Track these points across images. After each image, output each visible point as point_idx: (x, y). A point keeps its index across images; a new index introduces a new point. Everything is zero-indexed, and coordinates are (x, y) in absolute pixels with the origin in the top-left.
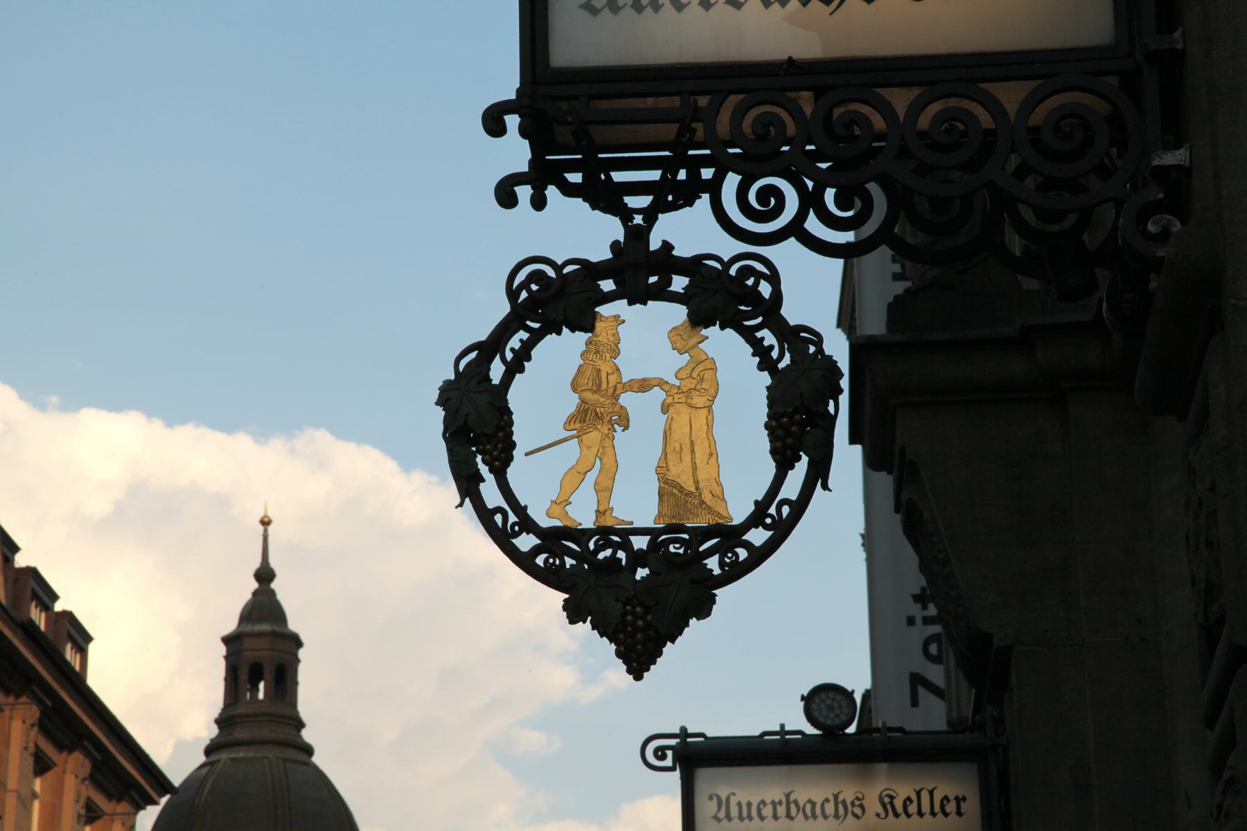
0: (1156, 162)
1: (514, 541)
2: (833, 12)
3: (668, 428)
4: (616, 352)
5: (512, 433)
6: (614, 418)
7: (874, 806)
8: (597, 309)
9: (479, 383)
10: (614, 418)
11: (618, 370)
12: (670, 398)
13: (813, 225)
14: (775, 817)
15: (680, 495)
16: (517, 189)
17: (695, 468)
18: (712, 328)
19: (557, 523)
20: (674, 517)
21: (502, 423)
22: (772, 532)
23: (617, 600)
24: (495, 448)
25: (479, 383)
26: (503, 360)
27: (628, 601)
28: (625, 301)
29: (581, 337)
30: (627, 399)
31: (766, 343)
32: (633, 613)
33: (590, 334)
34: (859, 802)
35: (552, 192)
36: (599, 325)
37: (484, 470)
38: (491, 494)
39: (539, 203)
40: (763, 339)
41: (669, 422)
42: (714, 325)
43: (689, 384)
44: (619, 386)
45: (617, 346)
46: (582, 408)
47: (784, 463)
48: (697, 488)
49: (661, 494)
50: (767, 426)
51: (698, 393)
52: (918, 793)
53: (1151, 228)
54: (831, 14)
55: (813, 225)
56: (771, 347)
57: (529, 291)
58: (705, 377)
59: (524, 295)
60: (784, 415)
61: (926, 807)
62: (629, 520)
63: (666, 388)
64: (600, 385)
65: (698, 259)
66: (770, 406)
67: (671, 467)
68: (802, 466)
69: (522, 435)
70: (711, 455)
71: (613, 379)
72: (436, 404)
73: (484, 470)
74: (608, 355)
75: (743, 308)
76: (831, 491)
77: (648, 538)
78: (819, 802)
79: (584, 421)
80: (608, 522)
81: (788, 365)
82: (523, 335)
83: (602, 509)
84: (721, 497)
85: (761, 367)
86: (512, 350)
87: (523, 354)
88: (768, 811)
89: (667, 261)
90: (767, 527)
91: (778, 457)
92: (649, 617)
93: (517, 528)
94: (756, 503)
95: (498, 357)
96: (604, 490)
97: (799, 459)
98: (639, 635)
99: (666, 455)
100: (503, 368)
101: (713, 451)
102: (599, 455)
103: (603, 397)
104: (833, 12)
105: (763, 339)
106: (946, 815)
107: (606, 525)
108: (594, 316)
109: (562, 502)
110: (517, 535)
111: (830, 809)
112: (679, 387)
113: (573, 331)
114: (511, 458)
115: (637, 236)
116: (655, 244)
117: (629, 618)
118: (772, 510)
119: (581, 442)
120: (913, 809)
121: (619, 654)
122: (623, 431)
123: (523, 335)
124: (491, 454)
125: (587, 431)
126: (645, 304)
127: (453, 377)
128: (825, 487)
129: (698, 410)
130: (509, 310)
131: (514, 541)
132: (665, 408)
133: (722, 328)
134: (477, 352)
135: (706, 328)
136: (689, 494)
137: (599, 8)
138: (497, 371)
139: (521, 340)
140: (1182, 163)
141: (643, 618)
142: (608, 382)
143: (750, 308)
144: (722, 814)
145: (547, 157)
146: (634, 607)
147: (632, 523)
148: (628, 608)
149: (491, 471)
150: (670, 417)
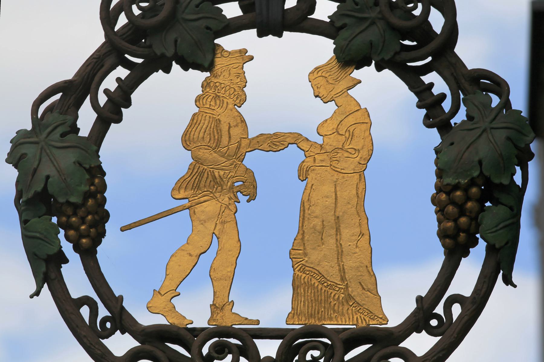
1: (105, 342)
3: (306, 200)
4: (242, 99)
5: (104, 200)
6: (236, 184)
8: (217, 41)
10: (236, 184)
11: (243, 121)
12: (311, 159)
15: (320, 286)
17: (340, 254)
18: (366, 68)
19: (160, 320)
20: (311, 316)
22: (439, 338)
24: (83, 220)
25: (63, 135)
26: (95, 104)
28: (255, 30)
31: (436, 91)
33: (208, 74)
36: (219, 62)
37: (67, 248)
40: (431, 85)
41: (308, 191)
42: (369, 65)
43: (334, 141)
44: (244, 143)
45: (243, 91)
46: (196, 170)
50: (434, 200)
51: (346, 154)
56: (443, 97)
57: (130, 14)
58: (356, 132)
59: (122, 20)
60: (456, 187)
62: (255, 318)
63: (305, 146)
64: (219, 141)
66: (440, 174)
67: (309, 250)
70: (362, 234)
72: (8, 161)
73: (67, 248)
74: (230, 101)
75: (407, 42)
76: (515, 286)
77: (279, 342)
79: (198, 188)
80: (226, 321)
81: (463, 122)
82: (122, 72)
83: (219, 303)
84: (374, 292)
85: (429, 122)
86: (107, 92)
90: (432, 332)
91: (447, 241)
93: (108, 325)
94: (419, 300)
95: (87, 102)
97: (475, 243)
100: (94, 116)
101: (365, 231)
103: (223, 156)
105: (431, 85)
107: (224, 324)
110: (109, 334)
112: (321, 146)
113: (186, 69)
114: (103, 234)
118: (439, 310)
122: (248, 201)
123: (122, 72)
124: (77, 229)
125: (202, 199)
126: (280, 35)
127: (29, 127)
128: (508, 281)
130: (103, 40)
131: (105, 342)
133: (379, 68)
134: (61, 94)
135: (358, 68)
139: (118, 80)
142: (230, 137)
143: (415, 43)
147: (258, 322)
149: (77, 248)
150: (310, 185)
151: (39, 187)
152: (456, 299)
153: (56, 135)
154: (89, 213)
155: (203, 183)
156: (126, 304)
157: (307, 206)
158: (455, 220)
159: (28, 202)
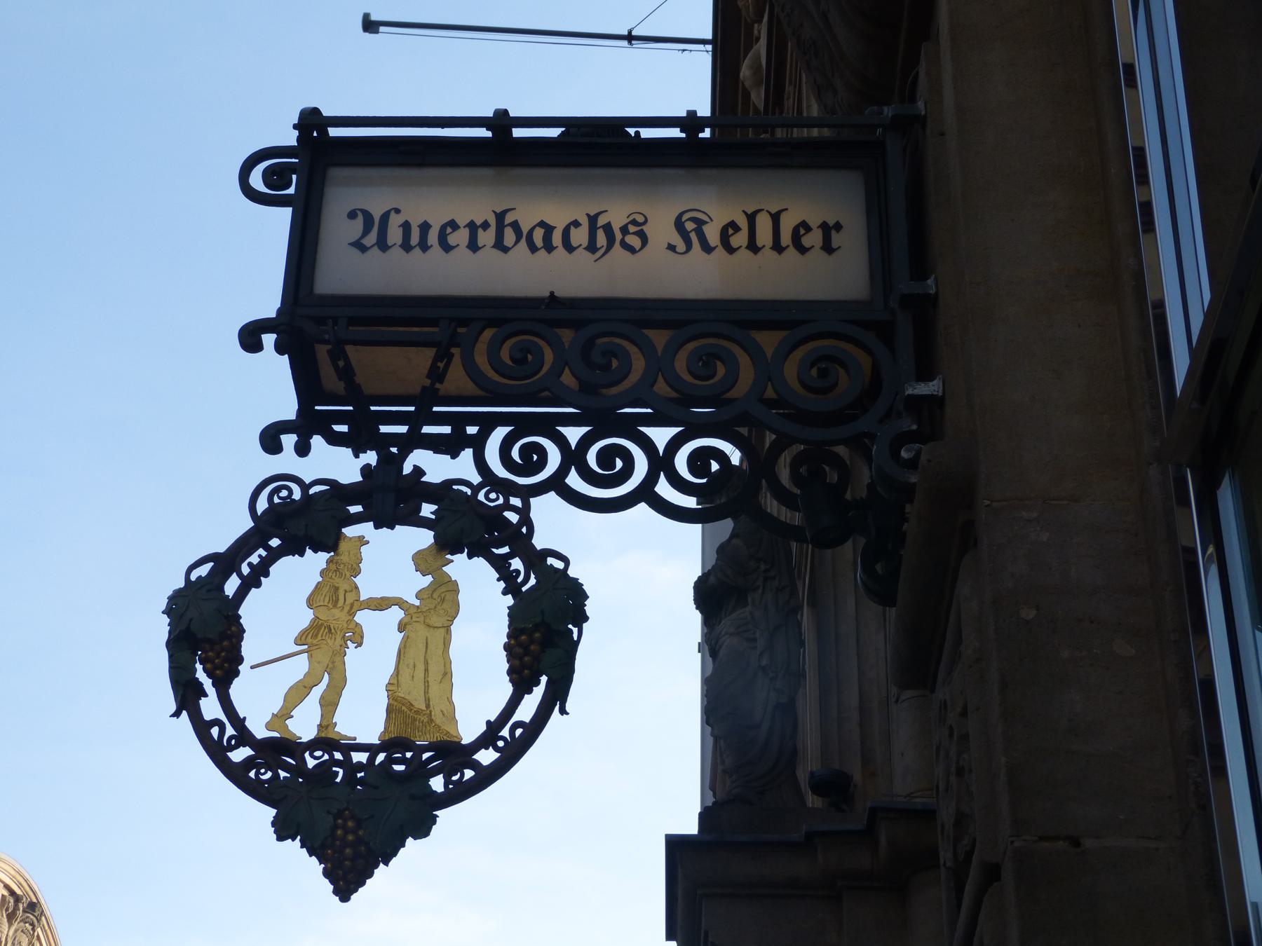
0: (909, 391)
2: (598, 259)
6: (347, 635)
8: (344, 530)
9: (209, 591)
11: (357, 588)
13: (574, 480)
15: (408, 712)
21: (229, 632)
23: (329, 812)
24: (218, 656)
25: (209, 591)
26: (240, 575)
27: (339, 814)
29: (323, 557)
30: (362, 617)
32: (344, 827)
35: (317, 441)
36: (343, 546)
37: (207, 683)
38: (210, 707)
39: (303, 449)
42: (462, 552)
46: (316, 624)
47: (522, 686)
48: (428, 706)
49: (389, 711)
53: (904, 454)
54: (595, 261)
55: (574, 480)
58: (446, 598)
60: (522, 631)
64: (337, 600)
65: (448, 484)
68: (539, 692)
69: (251, 649)
71: (350, 600)
76: (567, 714)
83: (325, 723)
86: (250, 565)
87: (261, 571)
89: (417, 488)
90: (497, 749)
91: (514, 676)
92: (361, 833)
93: (233, 742)
94: (488, 723)
96: (329, 704)
98: (348, 851)
99: (398, 672)
102: (328, 670)
104: (598, 259)
108: (339, 536)
109: (284, 714)
110: (232, 748)
113: (316, 552)
114: (237, 673)
115: (391, 463)
116: (407, 468)
118: (505, 732)
119: (310, 658)
121: (326, 873)
122: (356, 647)
128: (563, 711)
129: (436, 629)
132: (402, 627)
133: (470, 557)
136: (418, 712)
137: (368, 245)
138: (231, 586)
139: (260, 556)
140: (935, 393)
141: (354, 832)
145: (316, 408)
146: (345, 821)
148: (340, 821)
152: (519, 724)
154: (222, 651)
155: (320, 635)
156: (247, 724)
157: (402, 651)
158: (521, 659)
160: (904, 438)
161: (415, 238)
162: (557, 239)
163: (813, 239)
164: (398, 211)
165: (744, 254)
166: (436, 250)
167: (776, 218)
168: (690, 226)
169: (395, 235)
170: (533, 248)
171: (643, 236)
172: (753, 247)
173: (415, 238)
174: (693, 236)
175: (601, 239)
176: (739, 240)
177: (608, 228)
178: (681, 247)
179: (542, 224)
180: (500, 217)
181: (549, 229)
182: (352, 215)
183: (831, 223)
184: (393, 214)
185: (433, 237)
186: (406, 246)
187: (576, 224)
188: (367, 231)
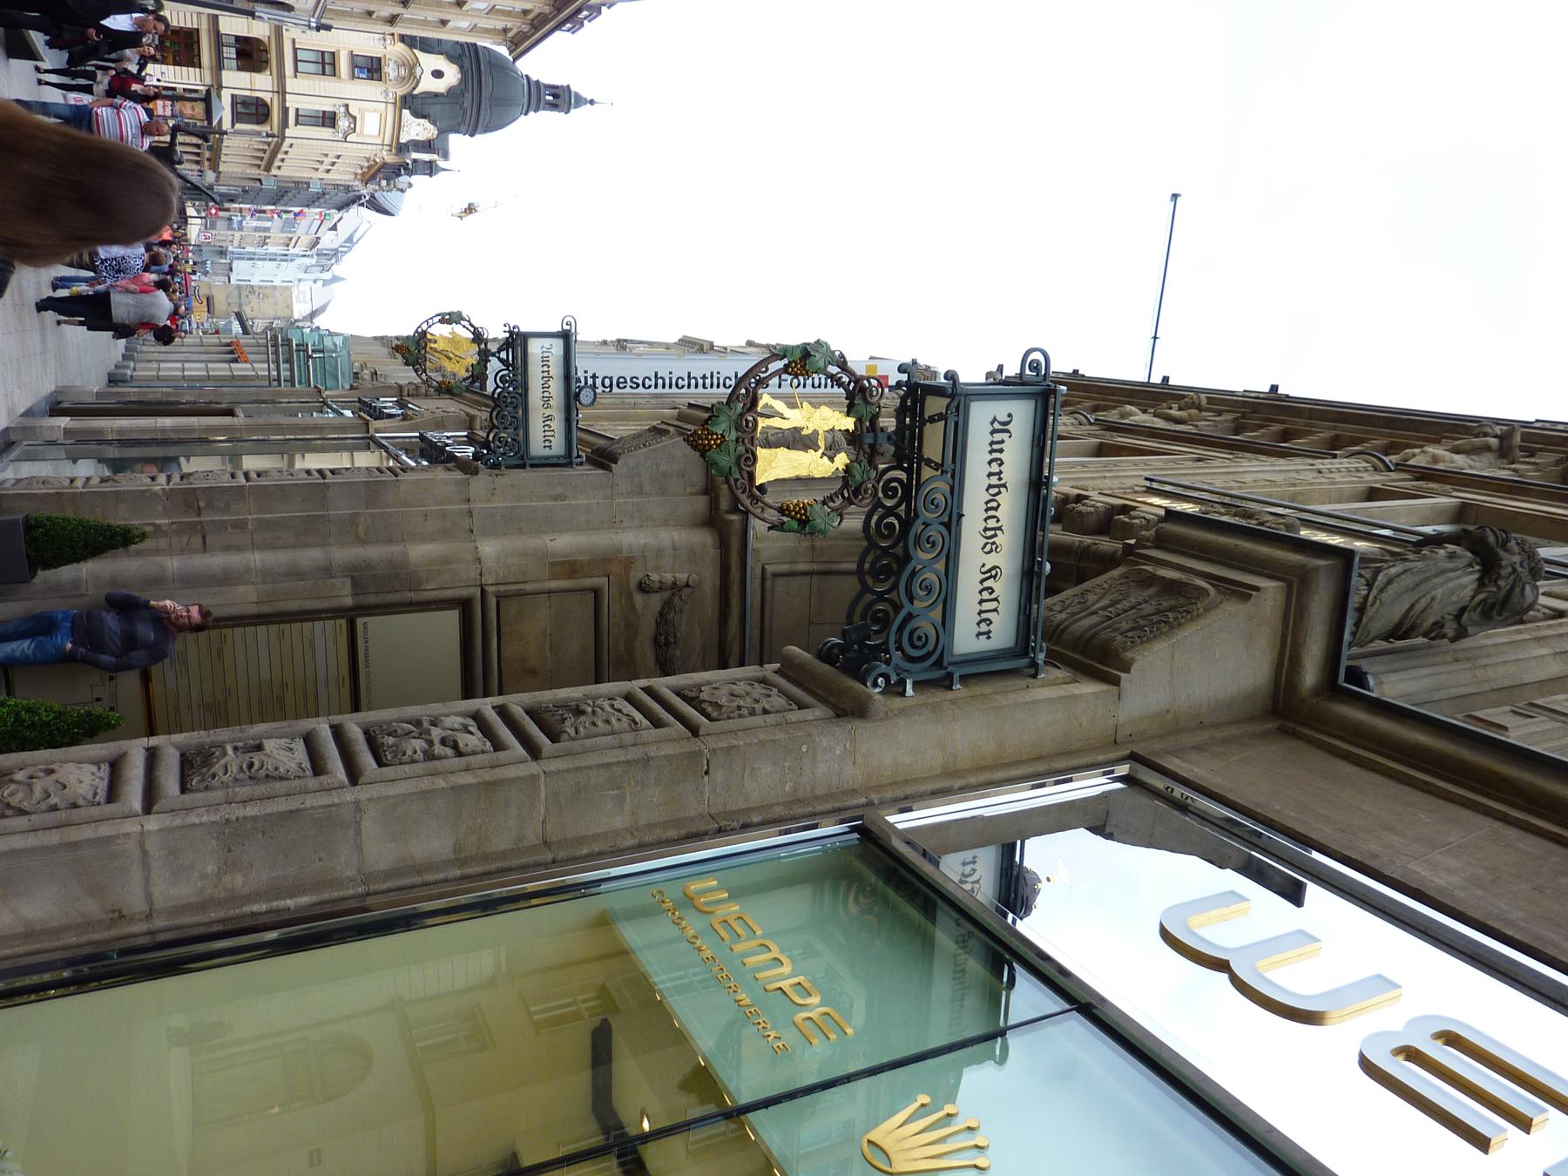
0: (908, 681)
7: (548, 412)
14: (543, 372)
16: (906, 375)
26: (838, 373)
27: (723, 436)
34: (549, 407)
52: (553, 431)
53: (880, 680)
60: (806, 511)
61: (547, 433)
78: (550, 390)
88: (545, 369)
95: (840, 370)
98: (707, 442)
106: (544, 441)
111: (546, 394)
117: (715, 437)
120: (547, 428)
144: (544, 349)
151: (812, 353)
153: (830, 359)
159: (806, 349)
160: (886, 677)
161: (995, 447)
162: (991, 513)
163: (984, 627)
164: (1010, 437)
165: (979, 598)
166: (990, 457)
167: (995, 610)
168: (993, 573)
169: (998, 437)
170: (987, 503)
171: (991, 551)
172: (981, 602)
173: (995, 447)
174: (989, 574)
175: (989, 533)
176: (986, 595)
177: (995, 535)
178: (983, 570)
179: (999, 505)
180: (1004, 486)
181: (996, 509)
182: (1010, 415)
183: (991, 635)
184: (1009, 434)
185: (996, 455)
186: (992, 443)
187: (998, 521)
188: (1000, 423)
